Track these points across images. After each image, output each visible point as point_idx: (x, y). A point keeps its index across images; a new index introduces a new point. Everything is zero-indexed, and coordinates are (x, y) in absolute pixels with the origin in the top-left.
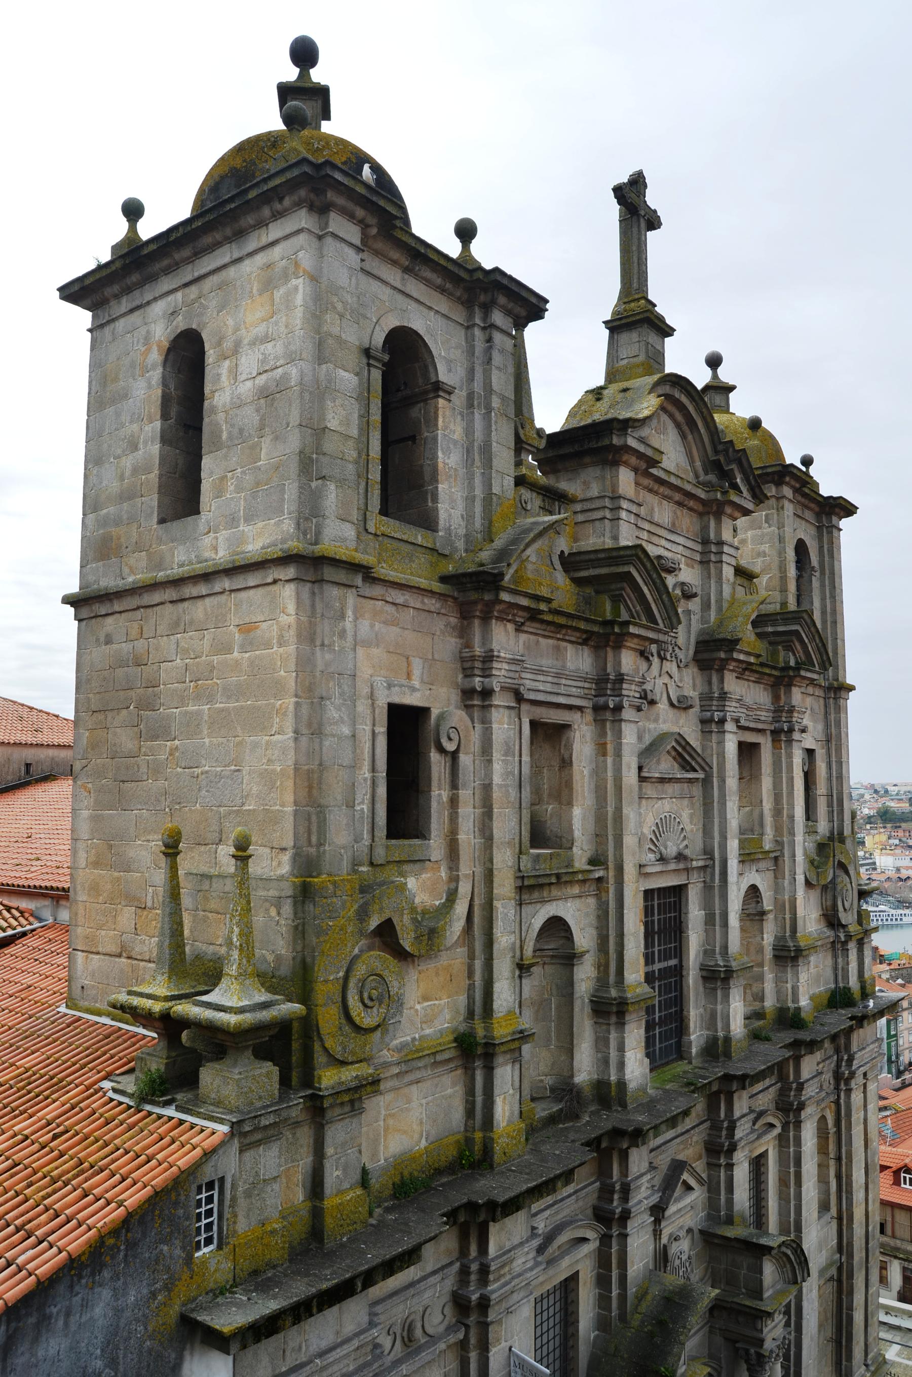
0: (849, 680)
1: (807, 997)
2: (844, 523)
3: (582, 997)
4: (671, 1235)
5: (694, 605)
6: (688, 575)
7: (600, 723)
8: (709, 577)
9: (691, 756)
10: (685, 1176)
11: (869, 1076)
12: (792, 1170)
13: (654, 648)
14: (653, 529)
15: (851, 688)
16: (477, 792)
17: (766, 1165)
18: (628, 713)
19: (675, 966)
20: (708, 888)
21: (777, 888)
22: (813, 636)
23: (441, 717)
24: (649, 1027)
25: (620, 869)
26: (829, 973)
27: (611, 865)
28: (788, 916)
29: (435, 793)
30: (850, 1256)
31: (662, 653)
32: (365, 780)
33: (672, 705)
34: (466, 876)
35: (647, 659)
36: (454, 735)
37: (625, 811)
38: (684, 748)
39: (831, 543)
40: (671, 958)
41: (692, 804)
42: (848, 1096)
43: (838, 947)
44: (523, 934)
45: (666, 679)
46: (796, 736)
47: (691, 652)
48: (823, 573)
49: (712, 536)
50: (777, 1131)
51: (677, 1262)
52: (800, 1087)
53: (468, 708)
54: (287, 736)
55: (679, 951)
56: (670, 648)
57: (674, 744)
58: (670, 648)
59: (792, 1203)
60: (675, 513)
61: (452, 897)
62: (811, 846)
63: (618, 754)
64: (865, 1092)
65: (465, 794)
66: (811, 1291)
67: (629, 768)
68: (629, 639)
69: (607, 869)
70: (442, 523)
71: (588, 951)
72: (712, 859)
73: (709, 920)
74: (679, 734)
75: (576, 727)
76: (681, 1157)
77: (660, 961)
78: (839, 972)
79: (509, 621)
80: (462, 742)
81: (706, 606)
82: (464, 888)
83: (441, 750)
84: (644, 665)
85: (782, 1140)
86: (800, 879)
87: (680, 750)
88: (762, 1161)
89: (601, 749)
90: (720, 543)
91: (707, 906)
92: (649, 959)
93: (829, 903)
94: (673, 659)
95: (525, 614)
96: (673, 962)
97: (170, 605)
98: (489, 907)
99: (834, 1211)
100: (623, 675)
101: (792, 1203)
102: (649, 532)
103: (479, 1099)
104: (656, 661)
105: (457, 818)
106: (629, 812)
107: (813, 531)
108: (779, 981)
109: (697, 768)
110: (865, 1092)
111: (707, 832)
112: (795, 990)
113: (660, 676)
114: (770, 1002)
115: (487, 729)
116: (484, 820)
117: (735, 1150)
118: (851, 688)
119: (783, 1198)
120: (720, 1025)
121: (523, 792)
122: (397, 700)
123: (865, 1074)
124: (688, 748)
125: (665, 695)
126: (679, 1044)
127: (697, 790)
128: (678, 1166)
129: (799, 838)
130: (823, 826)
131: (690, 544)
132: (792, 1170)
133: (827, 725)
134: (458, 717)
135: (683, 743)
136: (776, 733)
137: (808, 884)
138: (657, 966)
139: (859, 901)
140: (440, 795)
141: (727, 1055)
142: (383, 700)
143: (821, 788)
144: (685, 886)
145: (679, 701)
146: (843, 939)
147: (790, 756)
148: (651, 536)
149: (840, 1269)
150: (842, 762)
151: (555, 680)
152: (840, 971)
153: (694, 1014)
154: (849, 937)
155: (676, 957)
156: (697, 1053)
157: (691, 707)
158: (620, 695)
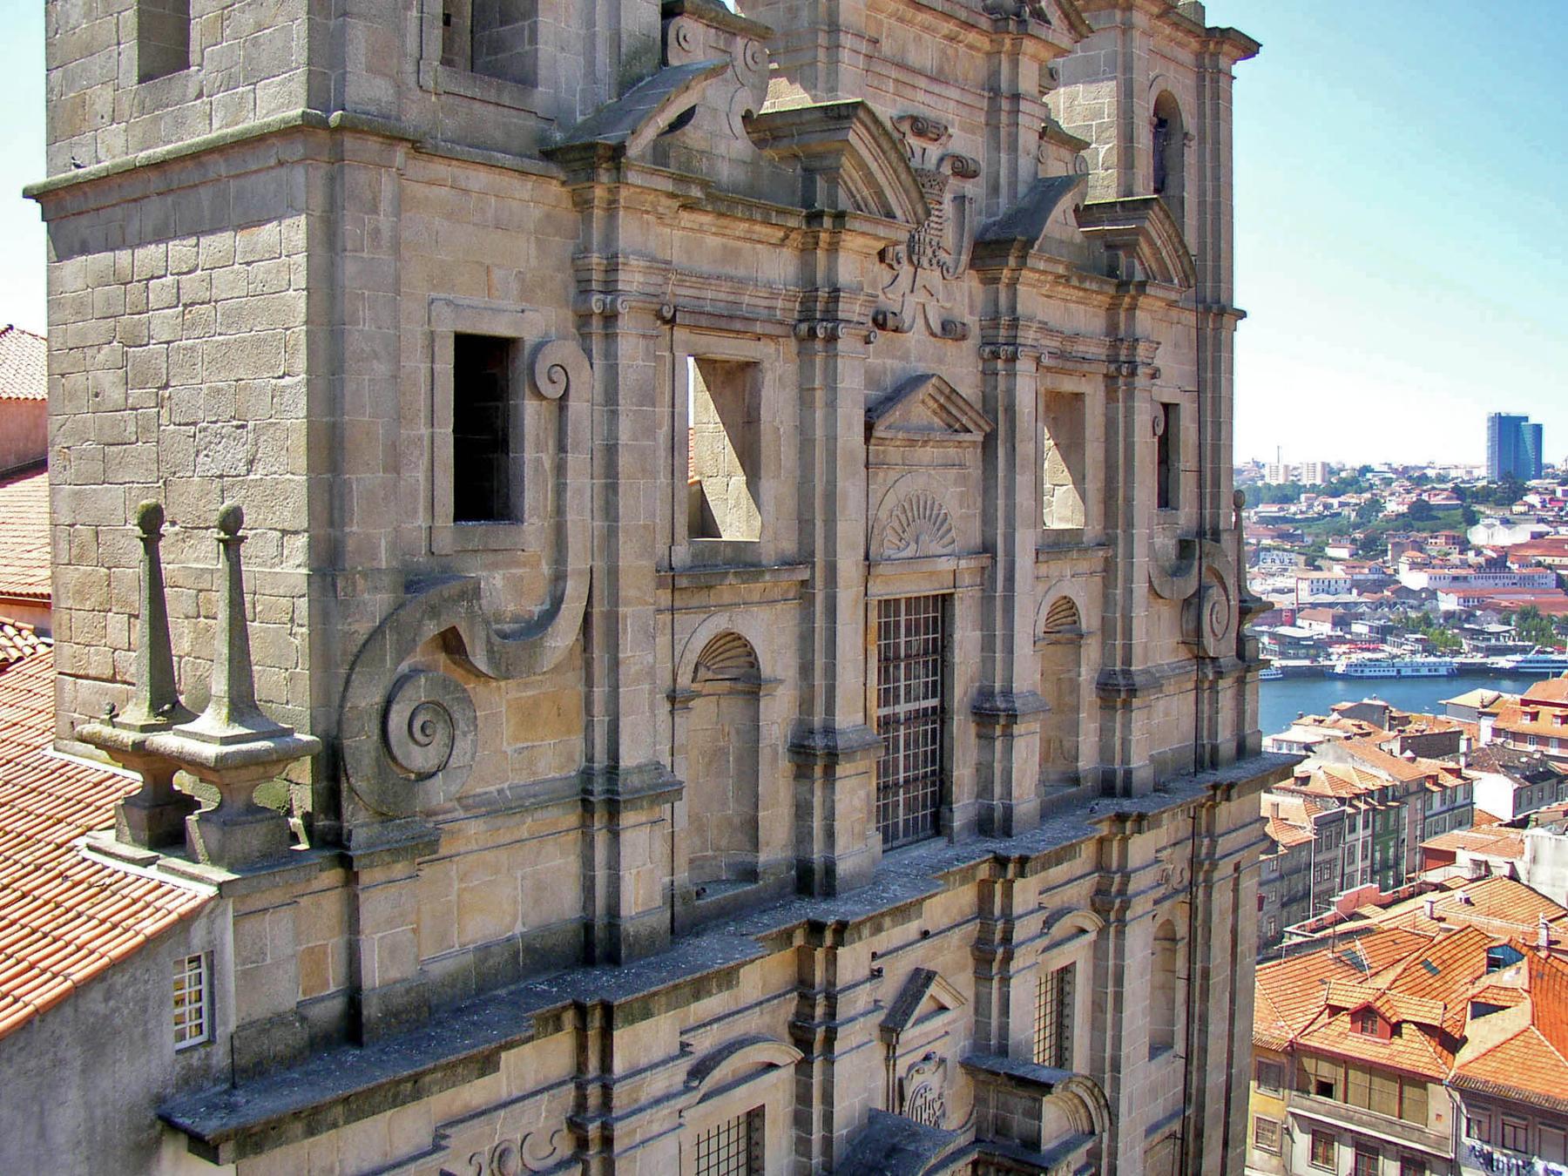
0: (1238, 303)
1: (1146, 755)
2: (1240, 69)
3: (774, 748)
4: (910, 1068)
5: (970, 188)
6: (965, 142)
7: (804, 355)
8: (998, 149)
9: (960, 409)
10: (933, 989)
11: (1242, 866)
12: (1110, 990)
13: (902, 249)
14: (903, 76)
15: (1242, 314)
16: (598, 455)
17: (1072, 983)
18: (847, 342)
19: (934, 708)
20: (987, 600)
21: (1107, 600)
22: (1169, 237)
23: (539, 348)
24: (884, 789)
25: (831, 569)
26: (1188, 724)
27: (819, 559)
28: (1119, 642)
29: (529, 454)
30: (1201, 1108)
31: (915, 258)
32: (420, 438)
33: (933, 334)
34: (580, 573)
35: (891, 267)
36: (558, 375)
37: (839, 484)
38: (948, 398)
39: (1216, 96)
40: (926, 697)
41: (962, 480)
42: (1209, 895)
43: (1204, 690)
44: (677, 660)
45: (921, 296)
46: (1141, 380)
47: (965, 258)
48: (1202, 141)
49: (1004, 86)
50: (1092, 936)
51: (919, 1102)
52: (1126, 877)
53: (585, 338)
54: (299, 378)
55: (940, 687)
56: (929, 252)
57: (931, 390)
58: (929, 252)
59: (1109, 1034)
60: (944, 52)
61: (557, 602)
62: (1166, 544)
63: (831, 405)
64: (1236, 890)
65: (576, 461)
66: (1132, 1148)
67: (850, 426)
68: (848, 238)
69: (813, 568)
70: (543, 73)
71: (781, 681)
72: (994, 558)
73: (988, 645)
74: (940, 378)
75: (766, 365)
76: (929, 966)
77: (908, 700)
78: (1203, 723)
79: (648, 212)
80: (572, 384)
81: (995, 189)
82: (575, 591)
83: (539, 395)
84: (887, 276)
85: (1098, 949)
86: (1140, 588)
87: (942, 400)
88: (1068, 977)
89: (805, 396)
90: (1016, 97)
91: (987, 625)
92: (887, 697)
93: (1192, 626)
94: (935, 266)
95: (676, 204)
96: (932, 702)
97: (155, 198)
98: (613, 619)
99: (1180, 1047)
100: (838, 290)
101: (1109, 1034)
102: (896, 81)
103: (601, 874)
104: (905, 270)
105: (565, 490)
106: (850, 489)
107: (1190, 81)
108: (1105, 732)
109: (971, 426)
110: (1236, 890)
111: (988, 519)
112: (1125, 743)
113: (912, 291)
114: (1087, 761)
115: (611, 366)
116: (607, 496)
117: (1012, 959)
118: (1242, 314)
119: (1097, 1026)
120: (998, 790)
121: (676, 457)
122: (468, 328)
123: (1237, 868)
124: (954, 397)
125: (920, 322)
126: (936, 817)
127: (973, 458)
128: (920, 980)
129: (1140, 532)
130: (1186, 515)
131: (968, 99)
132: (1110, 990)
133: (1200, 364)
134: (566, 351)
135: (947, 391)
136: (1110, 379)
137: (1154, 593)
138: (902, 708)
139: (1241, 623)
140: (539, 461)
141: (1007, 833)
142: (448, 326)
143: (1186, 459)
144: (952, 594)
145: (943, 326)
146: (1211, 678)
147: (1129, 412)
148: (900, 86)
149: (1185, 1121)
150: (1220, 423)
151: (732, 298)
152: (1206, 722)
153: (963, 774)
154: (1219, 674)
155: (934, 696)
156: (963, 827)
157: (964, 338)
158: (835, 320)
